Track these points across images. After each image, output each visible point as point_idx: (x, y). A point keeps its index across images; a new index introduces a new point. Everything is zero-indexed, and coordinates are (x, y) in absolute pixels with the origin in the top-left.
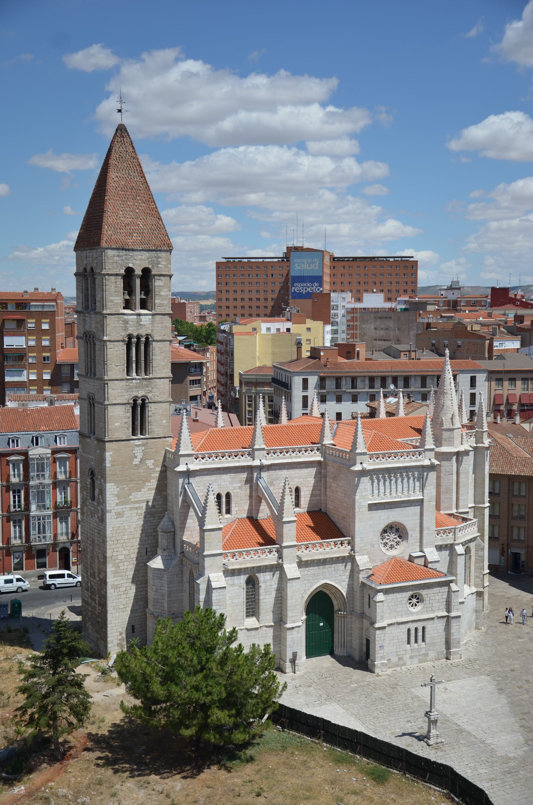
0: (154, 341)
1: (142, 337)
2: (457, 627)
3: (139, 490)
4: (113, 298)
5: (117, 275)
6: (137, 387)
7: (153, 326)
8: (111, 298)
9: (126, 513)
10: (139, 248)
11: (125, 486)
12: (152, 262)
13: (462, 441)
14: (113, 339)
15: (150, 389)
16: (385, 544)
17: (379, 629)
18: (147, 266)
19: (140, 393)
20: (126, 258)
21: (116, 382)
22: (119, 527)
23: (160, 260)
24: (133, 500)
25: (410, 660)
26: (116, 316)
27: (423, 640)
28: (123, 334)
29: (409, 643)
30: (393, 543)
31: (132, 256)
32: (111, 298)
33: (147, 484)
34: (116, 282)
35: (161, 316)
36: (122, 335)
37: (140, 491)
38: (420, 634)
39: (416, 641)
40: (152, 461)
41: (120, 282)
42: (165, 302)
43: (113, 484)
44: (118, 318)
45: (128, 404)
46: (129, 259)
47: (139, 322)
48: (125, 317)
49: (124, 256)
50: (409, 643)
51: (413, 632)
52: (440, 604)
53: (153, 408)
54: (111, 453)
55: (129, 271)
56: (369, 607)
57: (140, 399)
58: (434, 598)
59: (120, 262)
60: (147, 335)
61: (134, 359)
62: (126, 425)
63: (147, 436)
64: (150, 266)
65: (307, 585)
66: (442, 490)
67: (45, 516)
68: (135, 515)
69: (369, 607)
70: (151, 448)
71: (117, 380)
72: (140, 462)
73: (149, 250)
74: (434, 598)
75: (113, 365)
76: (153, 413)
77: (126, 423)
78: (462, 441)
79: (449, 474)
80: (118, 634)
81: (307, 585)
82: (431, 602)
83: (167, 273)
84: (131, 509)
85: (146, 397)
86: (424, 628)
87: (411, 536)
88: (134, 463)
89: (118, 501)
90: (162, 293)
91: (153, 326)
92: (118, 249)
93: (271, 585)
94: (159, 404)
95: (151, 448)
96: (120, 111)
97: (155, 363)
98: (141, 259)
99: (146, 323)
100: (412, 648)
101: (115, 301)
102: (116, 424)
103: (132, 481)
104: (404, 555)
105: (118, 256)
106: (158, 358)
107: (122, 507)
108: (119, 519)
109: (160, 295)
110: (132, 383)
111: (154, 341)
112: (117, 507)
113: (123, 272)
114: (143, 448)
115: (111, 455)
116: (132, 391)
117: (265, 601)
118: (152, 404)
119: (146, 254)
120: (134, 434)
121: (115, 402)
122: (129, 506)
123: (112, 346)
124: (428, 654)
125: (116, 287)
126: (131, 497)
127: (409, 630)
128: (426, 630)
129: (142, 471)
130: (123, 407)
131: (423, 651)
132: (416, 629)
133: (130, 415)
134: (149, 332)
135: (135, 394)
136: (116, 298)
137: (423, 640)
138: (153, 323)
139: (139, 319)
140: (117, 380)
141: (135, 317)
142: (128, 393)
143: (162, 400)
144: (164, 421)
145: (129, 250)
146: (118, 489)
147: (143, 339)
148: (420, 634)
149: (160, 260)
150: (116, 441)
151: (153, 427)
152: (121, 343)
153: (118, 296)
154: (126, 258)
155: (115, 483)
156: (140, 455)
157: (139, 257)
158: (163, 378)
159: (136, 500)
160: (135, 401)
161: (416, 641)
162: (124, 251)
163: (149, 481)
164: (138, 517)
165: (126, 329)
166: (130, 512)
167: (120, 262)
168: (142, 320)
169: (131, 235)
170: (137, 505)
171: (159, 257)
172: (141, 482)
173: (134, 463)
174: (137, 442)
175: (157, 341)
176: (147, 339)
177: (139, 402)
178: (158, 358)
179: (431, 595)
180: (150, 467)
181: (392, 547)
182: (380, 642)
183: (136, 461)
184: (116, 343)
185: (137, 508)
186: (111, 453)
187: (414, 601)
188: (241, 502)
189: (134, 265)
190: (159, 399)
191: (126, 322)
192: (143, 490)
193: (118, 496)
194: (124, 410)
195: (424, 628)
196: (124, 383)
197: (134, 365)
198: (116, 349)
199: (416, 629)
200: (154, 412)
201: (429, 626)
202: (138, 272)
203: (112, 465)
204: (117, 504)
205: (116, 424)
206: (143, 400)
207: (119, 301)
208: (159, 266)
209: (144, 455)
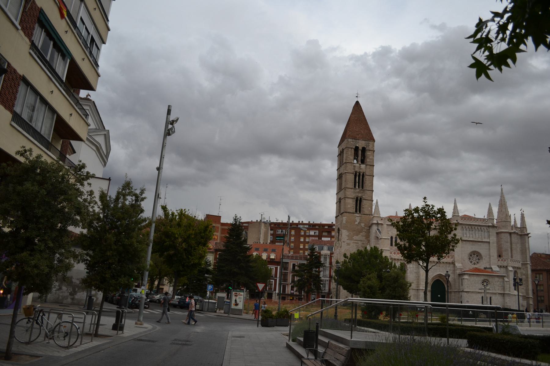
0: (366, 175)
1: (361, 173)
2: (509, 299)
3: (357, 235)
4: (350, 157)
5: (351, 148)
6: (358, 193)
8: (349, 157)
9: (351, 244)
11: (351, 232)
13: (512, 229)
14: (349, 172)
16: (471, 262)
17: (466, 292)
18: (364, 146)
19: (360, 195)
21: (349, 189)
22: (348, 249)
23: (369, 145)
24: (354, 239)
28: (353, 171)
30: (475, 262)
31: (358, 142)
32: (349, 157)
33: (361, 233)
34: (351, 151)
35: (369, 166)
36: (353, 171)
37: (358, 236)
40: (364, 224)
41: (353, 151)
42: (371, 161)
43: (346, 231)
45: (354, 198)
46: (357, 143)
47: (360, 167)
52: (499, 287)
53: (365, 202)
54: (346, 218)
56: (462, 285)
57: (359, 197)
58: (495, 284)
59: (353, 144)
60: (363, 172)
61: (357, 181)
62: (353, 207)
63: (362, 213)
64: (365, 147)
65: (431, 273)
66: (503, 250)
67: (326, 280)
68: (355, 245)
69: (462, 285)
70: (363, 219)
71: (350, 188)
72: (358, 223)
73: (365, 141)
74: (495, 284)
75: (348, 183)
76: (365, 204)
77: (353, 206)
78: (512, 229)
79: (507, 243)
80: (345, 297)
81: (431, 273)
82: (494, 285)
83: (372, 150)
84: (353, 243)
85: (362, 197)
86: (490, 298)
87: (484, 259)
88: (356, 223)
89: (348, 238)
90: (370, 157)
92: (353, 139)
93: (413, 270)
94: (368, 201)
95: (363, 219)
96: (357, 97)
97: (366, 184)
98: (362, 144)
102: (349, 206)
103: (355, 231)
104: (481, 268)
105: (352, 142)
106: (368, 182)
107: (350, 241)
108: (348, 246)
109: (369, 158)
110: (356, 190)
111: (366, 175)
112: (347, 241)
113: (354, 147)
114: (360, 218)
115: (346, 218)
117: (410, 277)
118: (364, 200)
119: (364, 142)
120: (356, 211)
121: (348, 197)
122: (352, 241)
126: (353, 238)
128: (492, 299)
129: (359, 227)
130: (352, 200)
133: (355, 203)
134: (364, 171)
135: (357, 195)
140: (350, 188)
141: (359, 165)
142: (354, 195)
143: (368, 199)
144: (370, 208)
145: (357, 140)
146: (348, 233)
148: (489, 300)
149: (369, 145)
150: (348, 213)
151: (365, 210)
152: (352, 174)
153: (352, 156)
154: (355, 143)
155: (347, 230)
156: (358, 221)
157: (361, 143)
158: (369, 190)
159: (356, 239)
160: (357, 198)
162: (355, 140)
163: (362, 232)
164: (356, 247)
165: (354, 169)
166: (353, 244)
167: (353, 144)
169: (358, 135)
170: (356, 242)
171: (369, 144)
172: (358, 232)
173: (356, 223)
174: (357, 215)
175: (367, 175)
176: (363, 174)
177: (359, 198)
178: (368, 182)
179: (494, 282)
180: (363, 227)
181: (474, 264)
183: (357, 223)
185: (356, 243)
186: (346, 218)
189: (359, 145)
191: (355, 166)
192: (359, 235)
193: (348, 236)
194: (352, 201)
195: (490, 298)
196: (353, 190)
197: (357, 184)
201: (493, 298)
202: (360, 148)
203: (346, 223)
204: (347, 240)
205: (349, 206)
206: (361, 198)
207: (352, 158)
208: (369, 147)
209: (360, 221)
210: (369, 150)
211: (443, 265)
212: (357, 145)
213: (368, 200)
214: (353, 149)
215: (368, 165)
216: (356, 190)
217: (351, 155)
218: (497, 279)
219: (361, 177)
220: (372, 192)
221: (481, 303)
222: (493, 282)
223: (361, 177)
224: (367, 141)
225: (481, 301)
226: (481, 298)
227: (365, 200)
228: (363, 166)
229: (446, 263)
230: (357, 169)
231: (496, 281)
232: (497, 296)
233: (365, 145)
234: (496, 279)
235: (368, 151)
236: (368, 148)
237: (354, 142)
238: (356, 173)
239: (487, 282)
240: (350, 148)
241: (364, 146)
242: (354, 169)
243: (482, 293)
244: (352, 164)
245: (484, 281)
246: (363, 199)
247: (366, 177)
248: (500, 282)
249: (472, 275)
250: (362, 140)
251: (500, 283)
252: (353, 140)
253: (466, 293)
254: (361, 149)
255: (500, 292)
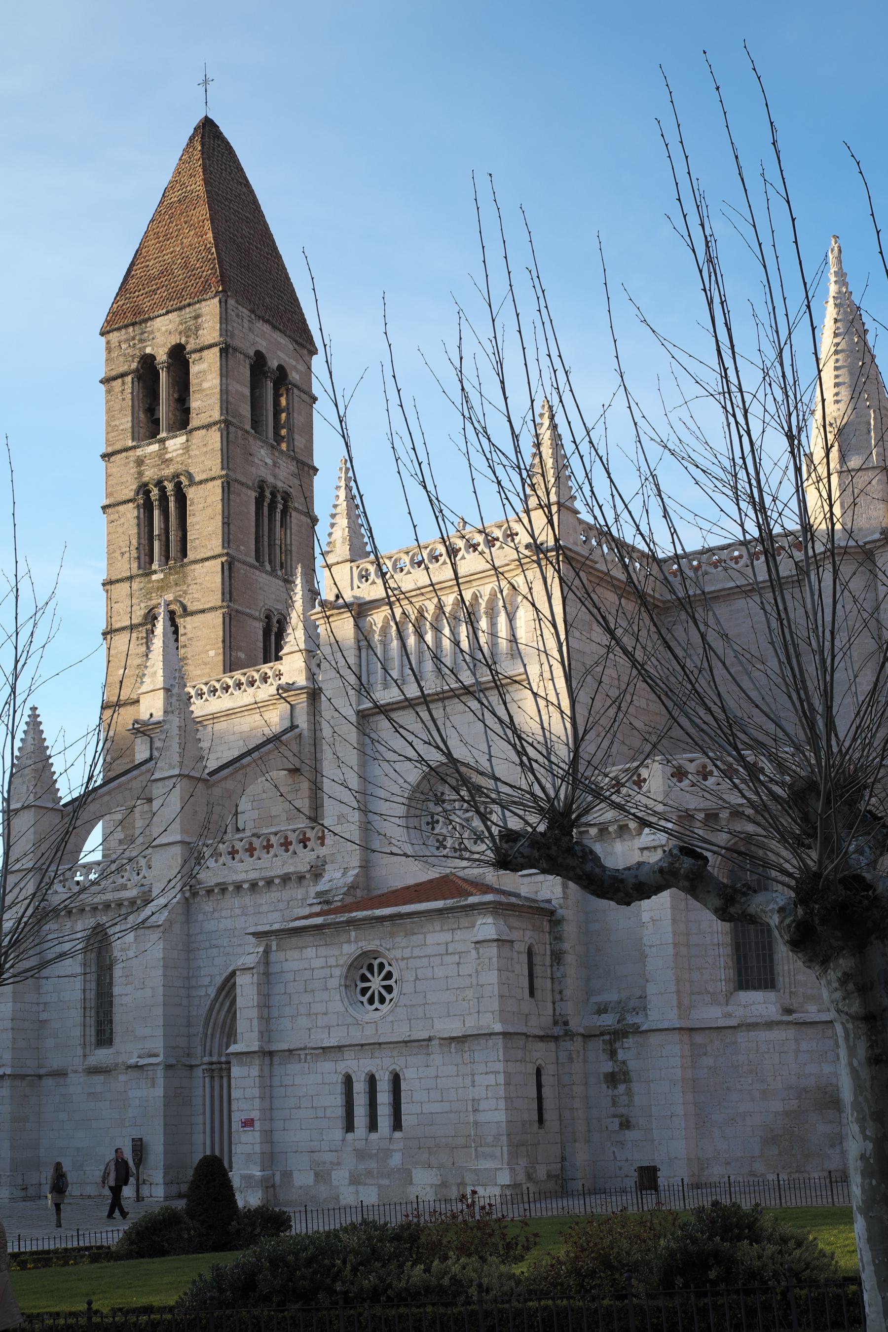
4: (117, 423)
5: (123, 375)
6: (163, 587)
7: (190, 457)
8: (114, 423)
10: (161, 312)
12: (187, 332)
15: (185, 588)
20: (141, 341)
23: (200, 320)
25: (352, 1189)
26: (124, 454)
27: (397, 1125)
28: (134, 487)
29: (349, 1127)
32: (114, 423)
38: (384, 1098)
39: (373, 1126)
44: (127, 458)
46: (145, 341)
48: (139, 452)
49: (137, 338)
50: (349, 1127)
51: (360, 1088)
55: (148, 361)
60: (178, 476)
64: (183, 341)
73: (180, 309)
91: (190, 457)
92: (126, 326)
99: (174, 454)
100: (361, 1145)
101: (121, 427)
109: (201, 391)
110: (150, 582)
116: (151, 600)
118: (188, 619)
123: (116, 516)
124: (409, 1173)
125: (124, 399)
127: (348, 1081)
128: (403, 1086)
131: (396, 1160)
132: (372, 1081)
136: (123, 421)
137: (397, 1125)
138: (186, 448)
139: (165, 448)
141: (155, 447)
145: (146, 321)
147: (169, 486)
148: (384, 1098)
157: (164, 329)
158: (207, 559)
161: (373, 1126)
162: (137, 328)
165: (140, 474)
168: (170, 450)
169: (154, 291)
171: (197, 317)
176: (178, 486)
182: (243, 1105)
184: (125, 506)
187: (376, 983)
188: (264, 796)
190: (201, 607)
195: (396, 1080)
198: (122, 520)
199: (372, 1081)
200: (189, 636)
202: (162, 356)
208: (200, 332)
210: (201, 350)
211: (274, 895)
212: (148, 350)
213: (203, 611)
214: (129, 379)
215: (198, 429)
216: (150, 582)
217: (121, 409)
218: (446, 937)
219: (172, 505)
220: (218, 562)
221: (340, 1123)
222: (413, 963)
223: (172, 505)
224: (189, 305)
225: (340, 1112)
226: (339, 1089)
227: (192, 614)
228: (175, 444)
229: (286, 879)
230: (150, 474)
231: (429, 956)
232: (437, 1058)
233: (180, 333)
234: (431, 939)
235: (193, 356)
236: (192, 340)
237: (133, 339)
238: (147, 493)
239: (387, 968)
240: (115, 378)
241: (174, 340)
242: (140, 474)
243: (347, 1055)
244: (131, 453)
245: (370, 968)
246: (181, 616)
247: (191, 493)
248: (456, 958)
249: (294, 940)
250: (168, 313)
251: (458, 964)
252: (131, 329)
253: (241, 1064)
254: (165, 358)
255: (454, 1028)
